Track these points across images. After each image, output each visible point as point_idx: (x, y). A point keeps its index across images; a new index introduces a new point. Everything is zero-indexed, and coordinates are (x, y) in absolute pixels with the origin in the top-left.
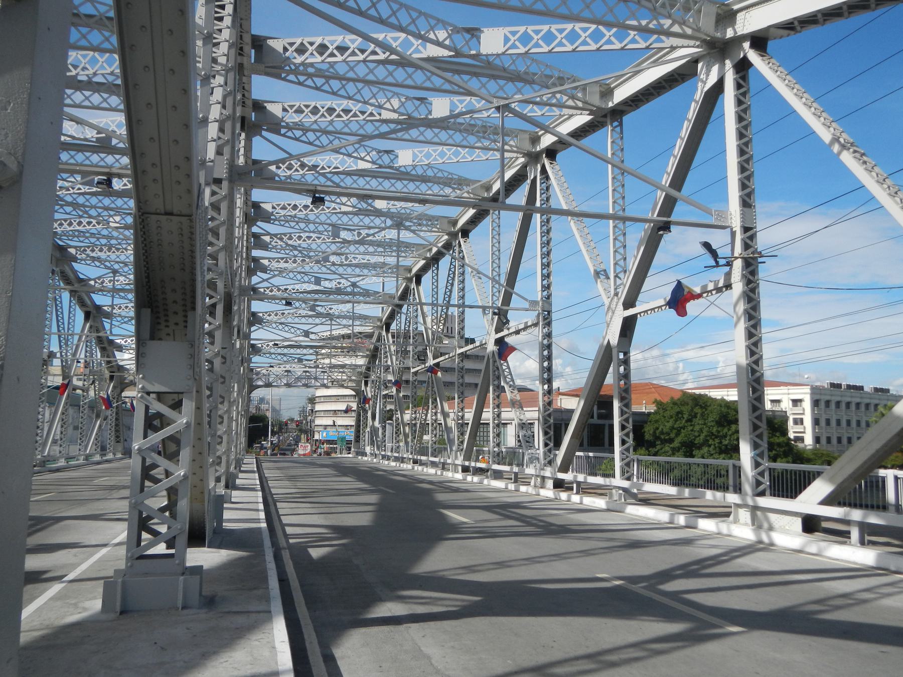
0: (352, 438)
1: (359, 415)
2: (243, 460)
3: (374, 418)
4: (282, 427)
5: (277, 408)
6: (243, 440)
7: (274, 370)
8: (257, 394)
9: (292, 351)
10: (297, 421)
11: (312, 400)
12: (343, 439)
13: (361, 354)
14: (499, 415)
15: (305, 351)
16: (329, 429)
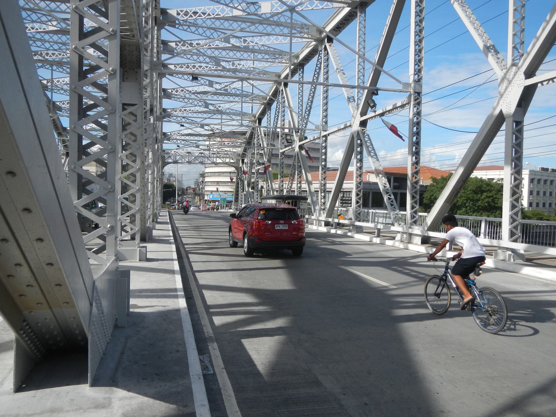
0: (233, 199)
1: (238, 184)
2: (159, 214)
3: (249, 186)
4: (184, 192)
5: (180, 179)
6: (159, 199)
7: (180, 151)
8: (169, 169)
9: (192, 138)
10: (193, 188)
11: (203, 175)
12: (224, 200)
13: (240, 141)
14: (325, 185)
15: (201, 138)
16: (214, 193)
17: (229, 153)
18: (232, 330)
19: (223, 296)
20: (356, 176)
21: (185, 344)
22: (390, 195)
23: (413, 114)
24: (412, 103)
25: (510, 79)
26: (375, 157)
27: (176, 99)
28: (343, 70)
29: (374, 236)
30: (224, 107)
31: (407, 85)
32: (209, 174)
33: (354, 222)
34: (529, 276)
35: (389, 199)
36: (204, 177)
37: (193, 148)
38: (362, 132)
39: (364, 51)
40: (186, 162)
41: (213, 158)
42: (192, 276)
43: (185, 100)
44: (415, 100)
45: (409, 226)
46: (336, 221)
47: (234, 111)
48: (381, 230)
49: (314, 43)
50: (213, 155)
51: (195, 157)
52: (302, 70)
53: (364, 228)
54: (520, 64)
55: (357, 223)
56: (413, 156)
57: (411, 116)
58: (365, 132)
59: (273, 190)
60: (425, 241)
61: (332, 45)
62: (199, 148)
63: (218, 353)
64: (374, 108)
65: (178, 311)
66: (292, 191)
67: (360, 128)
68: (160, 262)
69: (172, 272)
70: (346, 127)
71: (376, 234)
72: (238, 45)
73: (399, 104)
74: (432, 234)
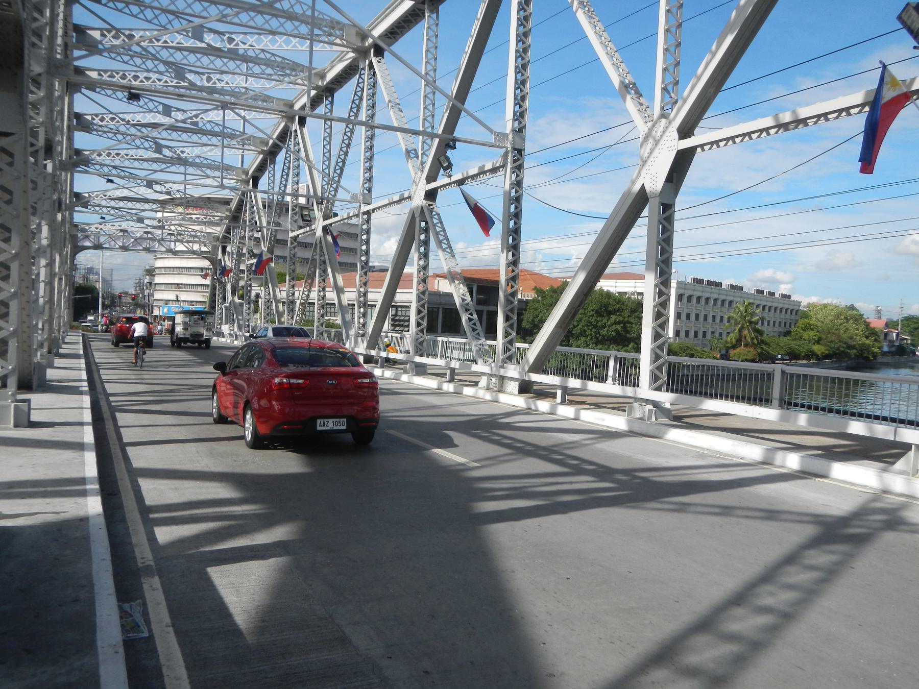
1: (214, 288)
2: (64, 338)
3: (234, 292)
4: (113, 301)
6: (64, 312)
7: (108, 228)
8: (85, 259)
9: (130, 205)
13: (219, 214)
14: (365, 294)
15: (147, 206)
16: (170, 304)
17: (199, 234)
18: (190, 552)
19: (176, 489)
20: (417, 282)
21: (92, 585)
22: (471, 314)
23: (511, 184)
24: (509, 166)
25: (657, 138)
26: (448, 250)
27: (100, 133)
28: (399, 104)
29: (445, 379)
30: (191, 152)
31: (502, 136)
32: (163, 270)
33: (413, 359)
34: (678, 443)
35: (470, 320)
36: (154, 275)
37: (132, 223)
38: (428, 209)
39: (435, 75)
40: (117, 246)
41: (169, 243)
42: (120, 454)
43: (117, 135)
44: (514, 161)
45: (500, 364)
46: (383, 354)
47: (210, 162)
48: (456, 371)
49: (352, 55)
50: (169, 237)
51: (136, 240)
52: (330, 99)
53: (428, 367)
54: (672, 116)
55: (418, 359)
56: (510, 251)
57: (507, 187)
58: (433, 208)
59: (277, 301)
60: (525, 388)
61: (383, 61)
62: (143, 222)
63: (160, 596)
64: (448, 171)
65: (84, 521)
66: (310, 303)
67: (425, 202)
68: (56, 428)
69: (80, 447)
70: (402, 200)
71: (448, 376)
72: (217, 46)
73: (489, 166)
74: (535, 377)
